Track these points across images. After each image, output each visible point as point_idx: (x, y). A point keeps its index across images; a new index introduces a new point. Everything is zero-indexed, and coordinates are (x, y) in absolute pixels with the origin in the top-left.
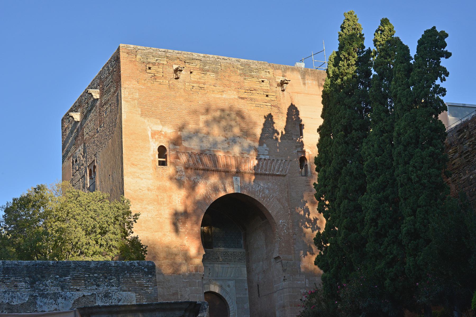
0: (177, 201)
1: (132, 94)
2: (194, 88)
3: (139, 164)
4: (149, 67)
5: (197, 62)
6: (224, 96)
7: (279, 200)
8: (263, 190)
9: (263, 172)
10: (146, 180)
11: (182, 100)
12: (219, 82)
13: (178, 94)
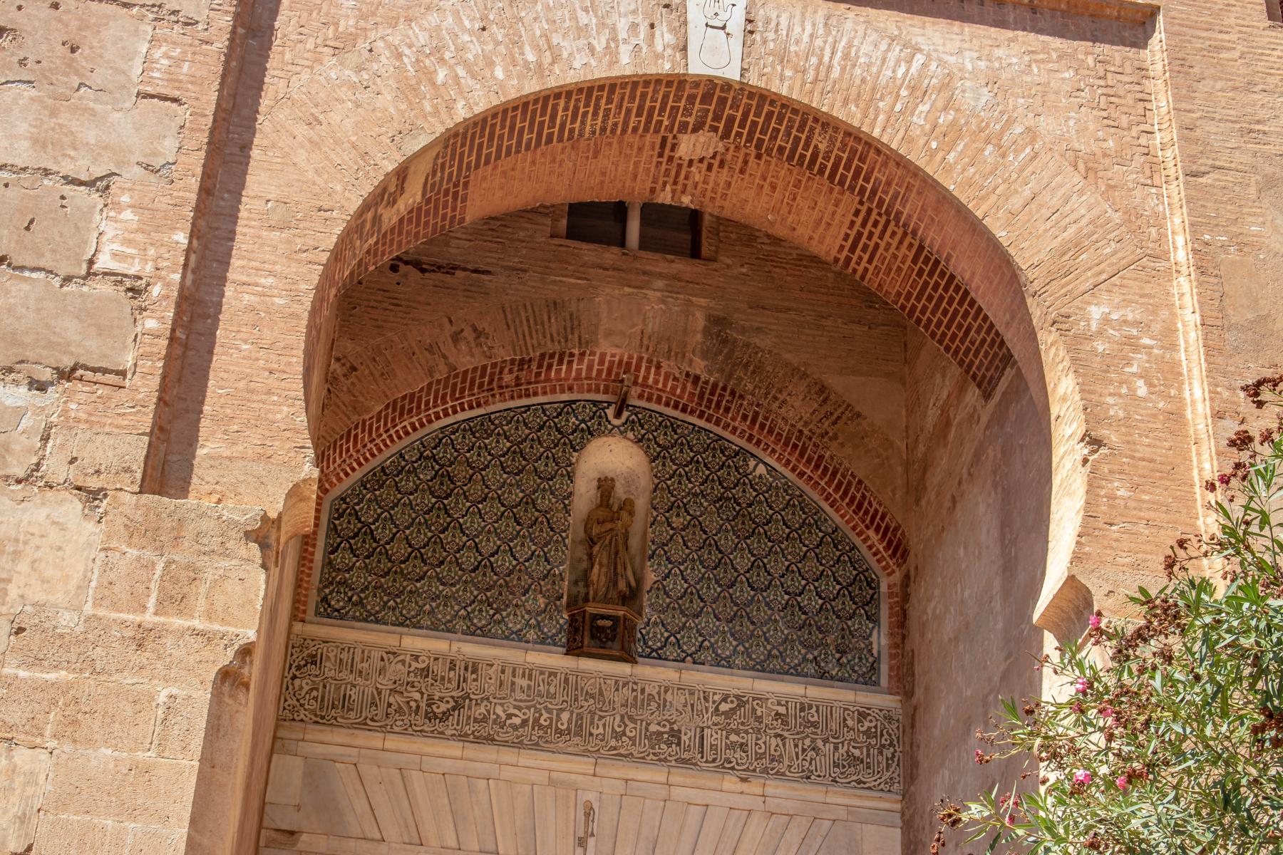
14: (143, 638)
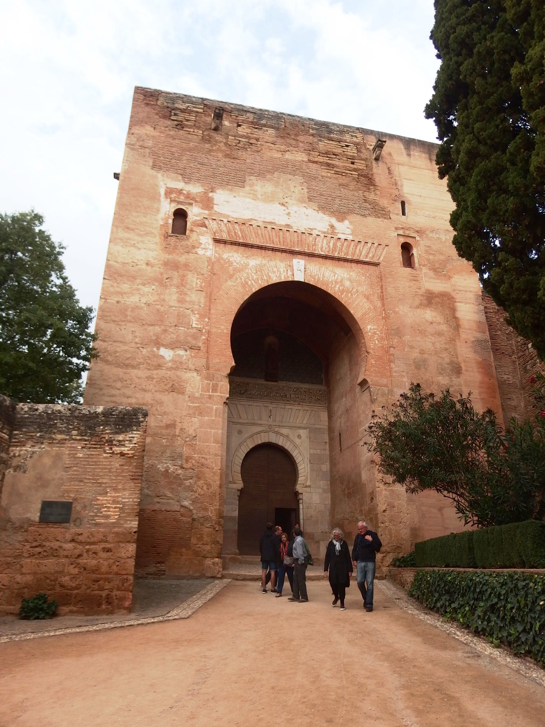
0: (194, 284)
1: (143, 141)
2: (242, 143)
3: (138, 229)
4: (174, 113)
5: (248, 115)
6: (288, 156)
7: (367, 297)
8: (341, 281)
9: (342, 255)
10: (146, 250)
12: (280, 140)
13: (214, 148)
14: (210, 397)
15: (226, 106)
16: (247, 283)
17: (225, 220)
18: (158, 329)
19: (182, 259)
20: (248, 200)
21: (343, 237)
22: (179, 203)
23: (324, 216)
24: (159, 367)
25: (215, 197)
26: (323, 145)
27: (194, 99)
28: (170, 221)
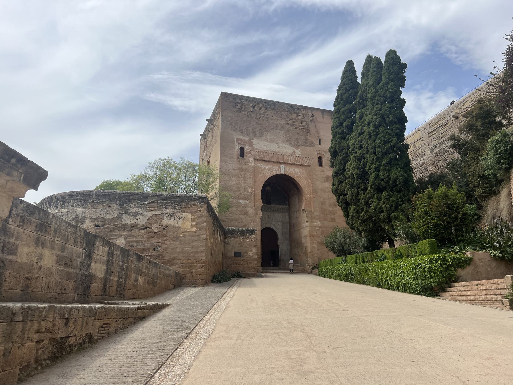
6: (278, 122)
7: (306, 179)
11: (254, 123)
14: (256, 216)
15: (255, 100)
16: (265, 175)
17: (257, 151)
18: (239, 193)
19: (244, 167)
20: (265, 142)
21: (298, 155)
22: (241, 144)
23: (291, 147)
24: (240, 206)
25: (253, 142)
26: (292, 116)
27: (243, 97)
28: (239, 152)
